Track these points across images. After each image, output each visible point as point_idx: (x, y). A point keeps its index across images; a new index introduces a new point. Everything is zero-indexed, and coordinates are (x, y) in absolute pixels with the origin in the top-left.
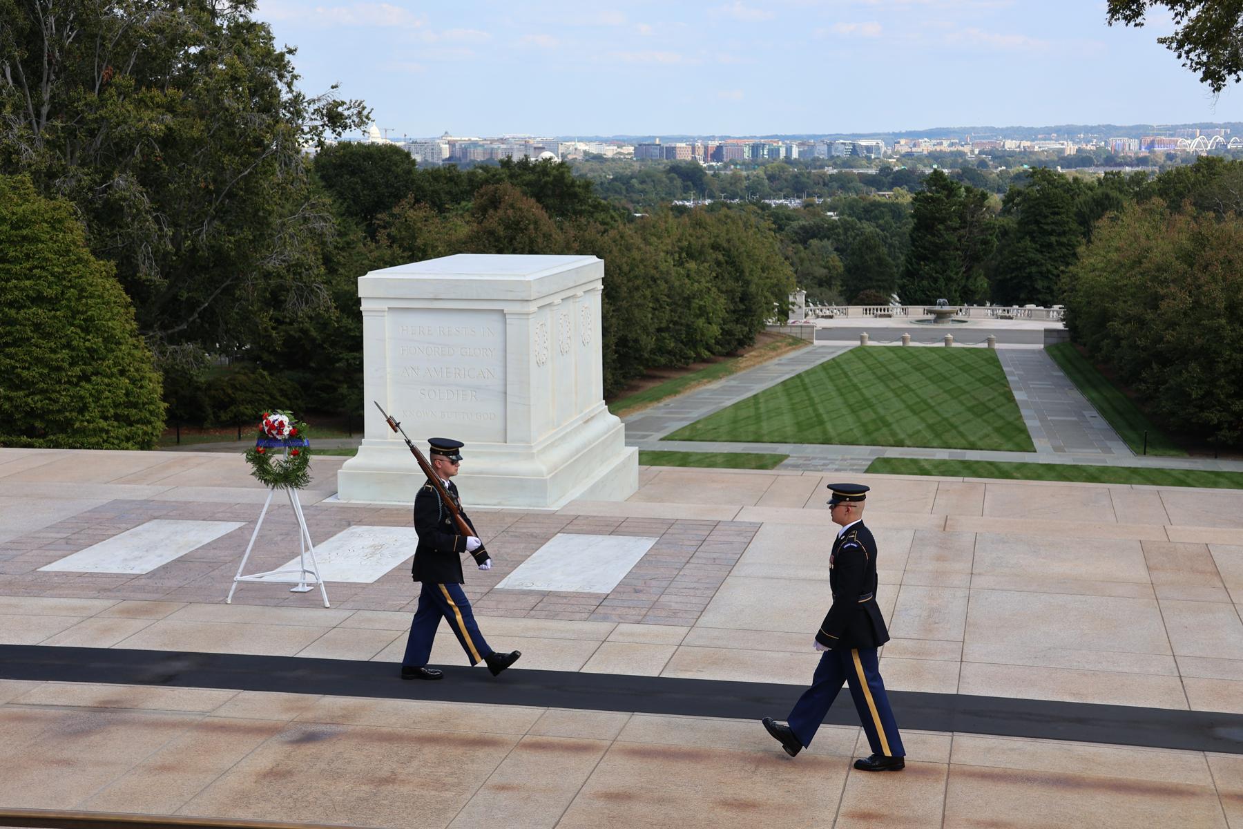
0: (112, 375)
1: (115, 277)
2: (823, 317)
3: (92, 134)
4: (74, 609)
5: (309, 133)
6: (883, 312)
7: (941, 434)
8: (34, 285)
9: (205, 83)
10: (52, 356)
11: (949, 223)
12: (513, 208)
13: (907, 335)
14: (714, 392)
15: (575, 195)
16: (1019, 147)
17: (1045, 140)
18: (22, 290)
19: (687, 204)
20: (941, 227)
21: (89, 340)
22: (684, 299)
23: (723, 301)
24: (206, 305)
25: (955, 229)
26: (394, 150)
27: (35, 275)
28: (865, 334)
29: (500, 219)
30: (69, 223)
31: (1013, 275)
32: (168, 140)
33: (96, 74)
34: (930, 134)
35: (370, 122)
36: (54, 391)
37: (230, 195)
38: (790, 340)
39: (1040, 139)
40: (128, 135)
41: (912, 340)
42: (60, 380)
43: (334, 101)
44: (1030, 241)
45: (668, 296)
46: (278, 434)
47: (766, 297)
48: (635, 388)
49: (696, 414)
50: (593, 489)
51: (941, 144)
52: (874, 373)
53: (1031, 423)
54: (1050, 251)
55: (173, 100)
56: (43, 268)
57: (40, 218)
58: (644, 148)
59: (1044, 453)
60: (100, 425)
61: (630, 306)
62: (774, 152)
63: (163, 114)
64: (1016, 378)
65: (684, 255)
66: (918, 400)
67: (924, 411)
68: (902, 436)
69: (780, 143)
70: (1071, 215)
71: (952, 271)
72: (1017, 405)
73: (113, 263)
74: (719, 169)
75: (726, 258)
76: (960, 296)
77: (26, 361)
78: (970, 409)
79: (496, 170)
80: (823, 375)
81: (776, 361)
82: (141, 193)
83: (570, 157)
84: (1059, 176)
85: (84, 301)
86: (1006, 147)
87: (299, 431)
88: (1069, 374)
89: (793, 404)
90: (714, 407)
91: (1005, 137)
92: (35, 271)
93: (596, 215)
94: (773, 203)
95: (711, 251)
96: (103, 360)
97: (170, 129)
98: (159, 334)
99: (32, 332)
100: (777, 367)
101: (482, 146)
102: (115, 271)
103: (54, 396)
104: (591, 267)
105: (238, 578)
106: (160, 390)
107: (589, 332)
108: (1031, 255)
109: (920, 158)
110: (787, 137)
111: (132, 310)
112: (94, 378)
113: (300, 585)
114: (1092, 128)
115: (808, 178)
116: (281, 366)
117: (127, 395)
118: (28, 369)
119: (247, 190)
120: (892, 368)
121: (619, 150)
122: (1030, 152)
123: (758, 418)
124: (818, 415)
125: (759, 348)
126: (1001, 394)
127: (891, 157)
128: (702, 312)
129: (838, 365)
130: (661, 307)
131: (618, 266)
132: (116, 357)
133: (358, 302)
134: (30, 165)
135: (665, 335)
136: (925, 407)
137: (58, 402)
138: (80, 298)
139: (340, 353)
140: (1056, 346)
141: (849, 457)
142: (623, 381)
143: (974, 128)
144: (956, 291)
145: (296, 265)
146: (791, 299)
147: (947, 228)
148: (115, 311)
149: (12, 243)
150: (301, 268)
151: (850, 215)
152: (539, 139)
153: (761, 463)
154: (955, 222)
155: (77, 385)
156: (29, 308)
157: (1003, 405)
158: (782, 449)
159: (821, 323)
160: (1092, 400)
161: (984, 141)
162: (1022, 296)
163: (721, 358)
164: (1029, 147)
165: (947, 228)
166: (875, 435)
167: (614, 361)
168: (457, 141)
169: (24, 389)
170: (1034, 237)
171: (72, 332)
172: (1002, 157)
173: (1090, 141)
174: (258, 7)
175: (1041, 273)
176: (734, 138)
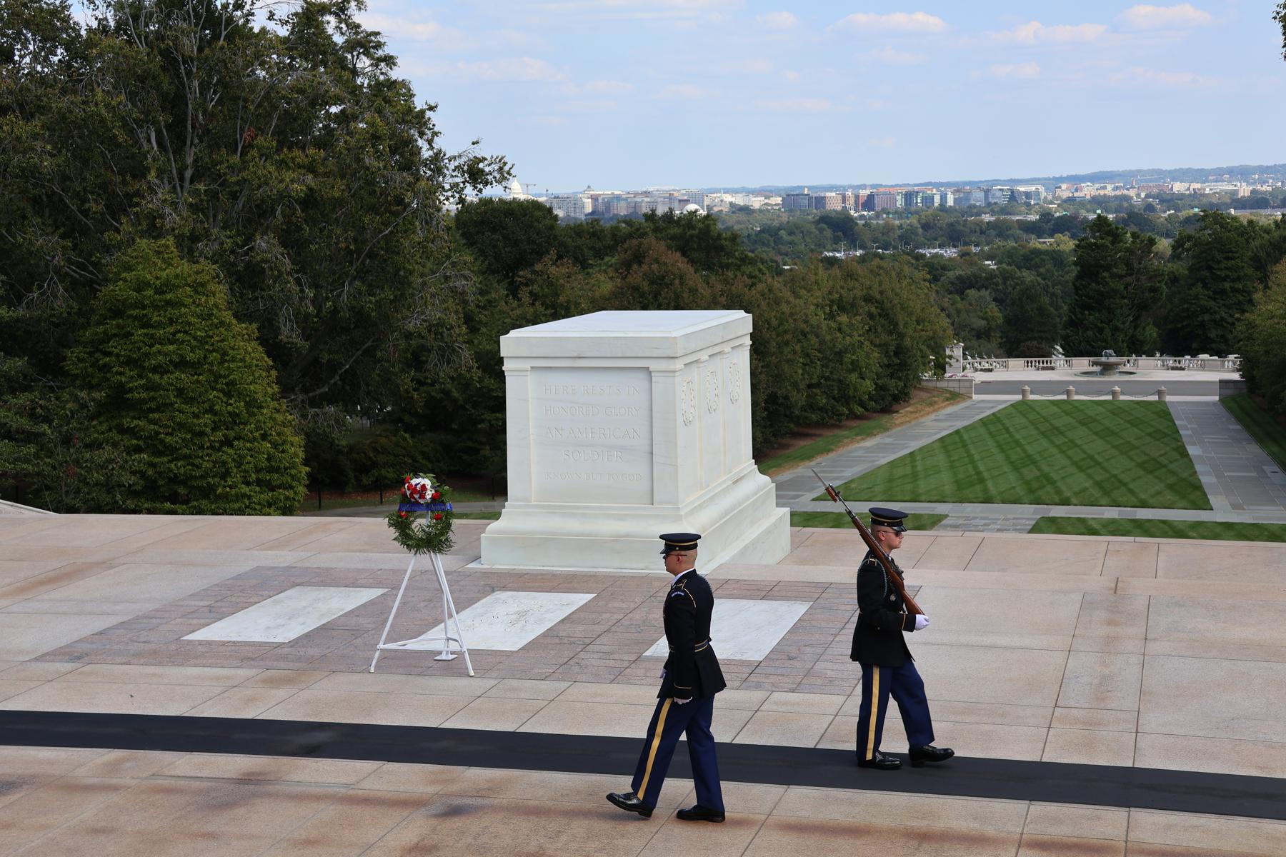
0: (254, 439)
1: (257, 339)
2: (981, 370)
3: (234, 196)
4: (217, 678)
5: (449, 190)
6: (1045, 365)
7: (1110, 492)
8: (178, 349)
9: (346, 142)
10: (195, 420)
11: (1114, 270)
12: (658, 262)
13: (1071, 388)
14: (867, 449)
15: (722, 248)
16: (1189, 189)
17: (1216, 181)
18: (166, 354)
19: (838, 255)
20: (1105, 274)
21: (231, 405)
22: (836, 353)
23: (876, 355)
24: (347, 367)
25: (1121, 277)
26: (534, 206)
27: (178, 340)
28: (1027, 388)
29: (645, 274)
30: (211, 287)
31: (1184, 323)
32: (310, 201)
34: (1093, 178)
35: (511, 177)
36: (197, 457)
37: (372, 255)
38: (948, 395)
39: (1211, 181)
41: (1077, 393)
42: (203, 446)
43: (475, 157)
44: (1202, 287)
45: (819, 352)
46: (420, 498)
47: (921, 351)
48: (787, 446)
49: (849, 473)
50: (743, 552)
51: (1105, 188)
52: (1037, 429)
53: (1207, 479)
54: (1224, 298)
55: (314, 160)
56: (186, 332)
57: (183, 282)
58: (792, 198)
59: (1221, 510)
60: (243, 491)
61: (780, 361)
62: (928, 200)
63: (304, 175)
64: (1189, 432)
65: (835, 308)
66: (1085, 456)
67: (1090, 467)
68: (1068, 494)
69: (934, 191)
70: (1246, 260)
71: (1118, 321)
72: (1191, 461)
73: (254, 326)
74: (870, 218)
75: (879, 311)
76: (1127, 347)
77: (169, 427)
78: (1141, 465)
80: (982, 431)
81: (933, 416)
82: (282, 254)
83: (716, 209)
84: (1232, 218)
85: (226, 365)
86: (1175, 190)
87: (442, 495)
88: (1247, 427)
89: (951, 462)
90: (867, 466)
91: (1174, 179)
92: (180, 336)
93: (743, 268)
94: (928, 252)
95: (863, 303)
96: (245, 424)
97: (311, 189)
98: (301, 397)
99: (175, 397)
100: (934, 422)
101: (626, 199)
102: (257, 334)
103: (197, 461)
104: (739, 322)
105: (381, 646)
106: (302, 455)
107: (738, 389)
108: (1202, 302)
109: (1082, 203)
110: (941, 184)
111: (274, 373)
112: (236, 443)
113: (444, 653)
114: (1268, 167)
115: (964, 226)
116: (423, 428)
117: (269, 459)
118: (171, 434)
119: (387, 250)
120: (1057, 423)
121: (766, 201)
122: (1201, 195)
123: (915, 477)
124: (979, 473)
125: (914, 404)
126: (1173, 449)
127: (1052, 203)
128: (855, 366)
129: (999, 420)
130: (811, 361)
131: (767, 321)
132: (258, 421)
133: (500, 361)
134: (173, 229)
135: (817, 391)
136: (1092, 463)
137: (201, 468)
138: (222, 362)
139: (483, 414)
140: (1233, 398)
141: (1013, 516)
142: (773, 439)
143: (1139, 171)
144: (1123, 341)
145: (437, 325)
146: (948, 352)
147: (1113, 276)
148: (257, 375)
149: (156, 307)
151: (1009, 264)
152: (684, 192)
154: (1121, 270)
155: (219, 450)
156: (172, 373)
157: (1176, 460)
158: (940, 508)
159: (980, 377)
160: (1274, 456)
161: (1150, 184)
162: (1194, 345)
163: (875, 415)
164: (1199, 189)
165: (1113, 276)
166: (1040, 493)
167: (763, 419)
168: (600, 195)
169: (167, 455)
170: (1207, 284)
171: (214, 397)
172: (1170, 200)
173: (1265, 182)
174: (399, 64)
175: (1215, 321)
176: (886, 186)
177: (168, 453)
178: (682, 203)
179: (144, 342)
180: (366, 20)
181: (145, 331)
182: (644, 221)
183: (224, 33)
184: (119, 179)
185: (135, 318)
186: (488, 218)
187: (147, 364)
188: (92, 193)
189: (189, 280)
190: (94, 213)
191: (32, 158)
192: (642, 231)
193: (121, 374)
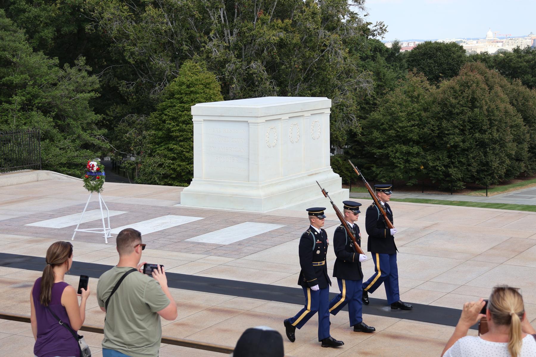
9: (299, 16)
26: (454, 45)
29: (458, 81)
30: (212, 86)
32: (281, 44)
33: (255, 14)
35: (386, 32)
40: (262, 42)
43: (367, 22)
55: (287, 25)
77: (188, 149)
79: (510, 53)
82: (263, 70)
97: (282, 39)
105: (76, 230)
116: (359, 157)
134: (216, 58)
139: (373, 150)
145: (340, 105)
149: (186, 94)
150: (343, 106)
169: (186, 162)
177: (186, 160)
179: (180, 110)
181: (181, 105)
182: (513, 52)
184: (198, 35)
185: (179, 99)
186: (428, 52)
187: (180, 120)
188: (185, 41)
189: (203, 82)
190: (185, 50)
191: (158, 25)
192: (510, 58)
193: (170, 124)
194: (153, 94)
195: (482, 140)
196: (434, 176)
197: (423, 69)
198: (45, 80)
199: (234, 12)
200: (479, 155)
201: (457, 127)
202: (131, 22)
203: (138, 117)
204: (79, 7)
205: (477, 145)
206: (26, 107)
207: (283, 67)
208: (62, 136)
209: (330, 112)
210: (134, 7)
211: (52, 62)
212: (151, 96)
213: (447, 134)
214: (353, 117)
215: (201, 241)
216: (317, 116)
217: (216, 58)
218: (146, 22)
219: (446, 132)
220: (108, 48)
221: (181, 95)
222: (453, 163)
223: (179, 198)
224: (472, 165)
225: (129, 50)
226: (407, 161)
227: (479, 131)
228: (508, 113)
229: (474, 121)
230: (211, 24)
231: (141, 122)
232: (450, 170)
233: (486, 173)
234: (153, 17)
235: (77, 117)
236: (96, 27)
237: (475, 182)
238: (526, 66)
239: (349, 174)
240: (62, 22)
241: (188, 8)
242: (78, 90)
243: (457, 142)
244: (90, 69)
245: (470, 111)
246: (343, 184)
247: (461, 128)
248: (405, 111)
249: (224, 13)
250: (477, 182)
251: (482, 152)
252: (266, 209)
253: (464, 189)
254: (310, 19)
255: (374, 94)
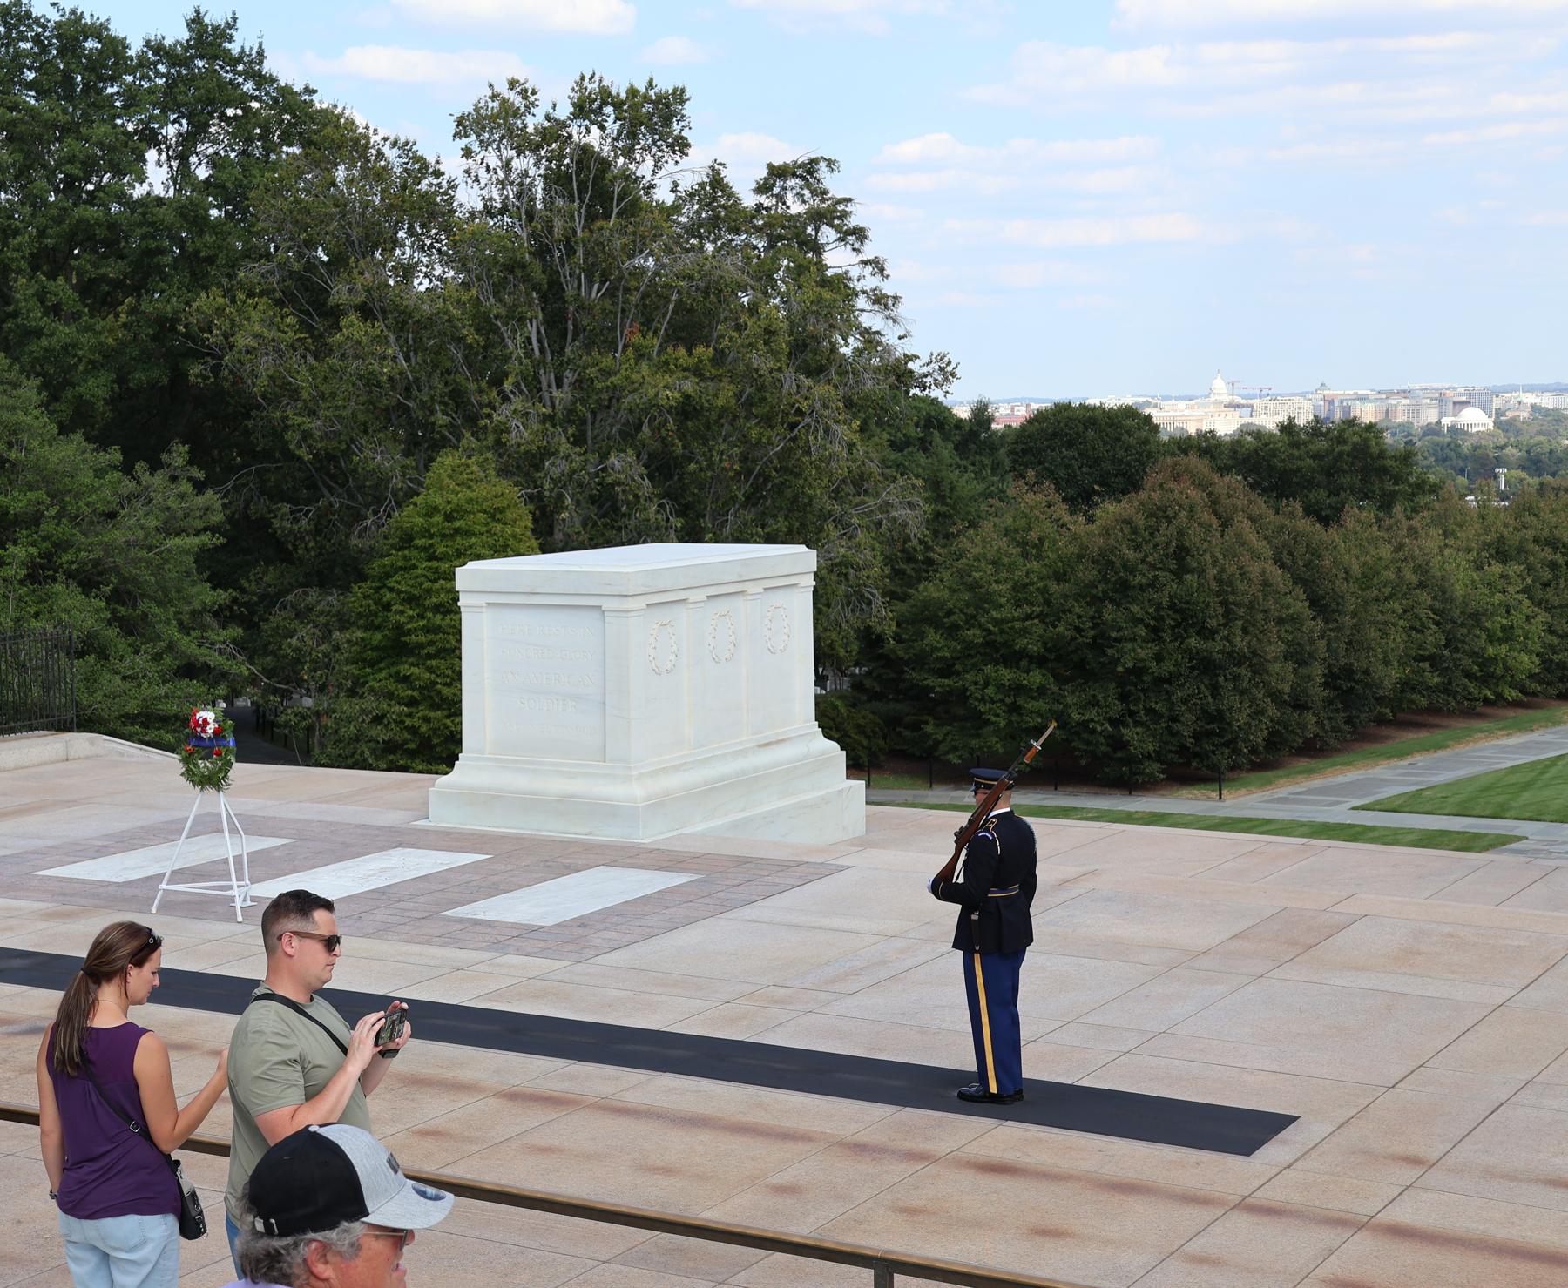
9: (731, 339)
26: (1130, 412)
29: (1142, 504)
30: (510, 515)
32: (687, 410)
33: (619, 333)
40: (638, 405)
43: (905, 355)
48: (1387, 738)
55: (701, 361)
77: (448, 676)
79: (1271, 435)
90: (1485, 768)
97: (687, 397)
105: (164, 886)
116: (891, 696)
130: (1423, 625)
134: (519, 445)
135: (1426, 665)
139: (926, 679)
145: (840, 564)
149: (444, 536)
153: (1469, 843)
169: (444, 709)
178: (1458, 406)
180: (835, 185)
181: (430, 564)
182: (1278, 433)
183: (616, 210)
184: (474, 386)
185: (424, 549)
187: (427, 602)
188: (441, 403)
190: (441, 426)
192: (1271, 446)
193: (402, 613)
194: (360, 536)
195: (1205, 654)
196: (1085, 747)
197: (1052, 473)
198: (88, 504)
199: (566, 329)
200: (1199, 693)
201: (1141, 621)
202: (304, 357)
203: (320, 595)
204: (175, 320)
205: (1193, 668)
206: (39, 573)
207: (692, 466)
208: (129, 645)
209: (814, 583)
210: (312, 318)
211: (104, 458)
212: (354, 541)
213: (1116, 640)
214: (874, 596)
215: (481, 917)
216: (780, 593)
217: (519, 445)
218: (342, 355)
219: (1114, 634)
220: (246, 422)
221: (431, 538)
222: (1132, 714)
223: (426, 803)
224: (1182, 719)
225: (299, 425)
226: (1015, 709)
227: (1198, 633)
228: (1271, 585)
229: (1184, 606)
230: (507, 358)
231: (328, 609)
232: (1125, 731)
233: (1216, 740)
234: (359, 342)
235: (166, 596)
236: (216, 369)
237: (1188, 764)
238: (1313, 469)
239: (865, 743)
240: (132, 359)
241: (449, 321)
242: (169, 529)
243: (1142, 660)
244: (198, 474)
245: (1173, 581)
246: (848, 767)
247: (1152, 623)
248: (1006, 580)
249: (539, 332)
250: (1194, 764)
251: (1206, 686)
252: (648, 835)
253: (1162, 780)
254: (761, 345)
255: (925, 536)
